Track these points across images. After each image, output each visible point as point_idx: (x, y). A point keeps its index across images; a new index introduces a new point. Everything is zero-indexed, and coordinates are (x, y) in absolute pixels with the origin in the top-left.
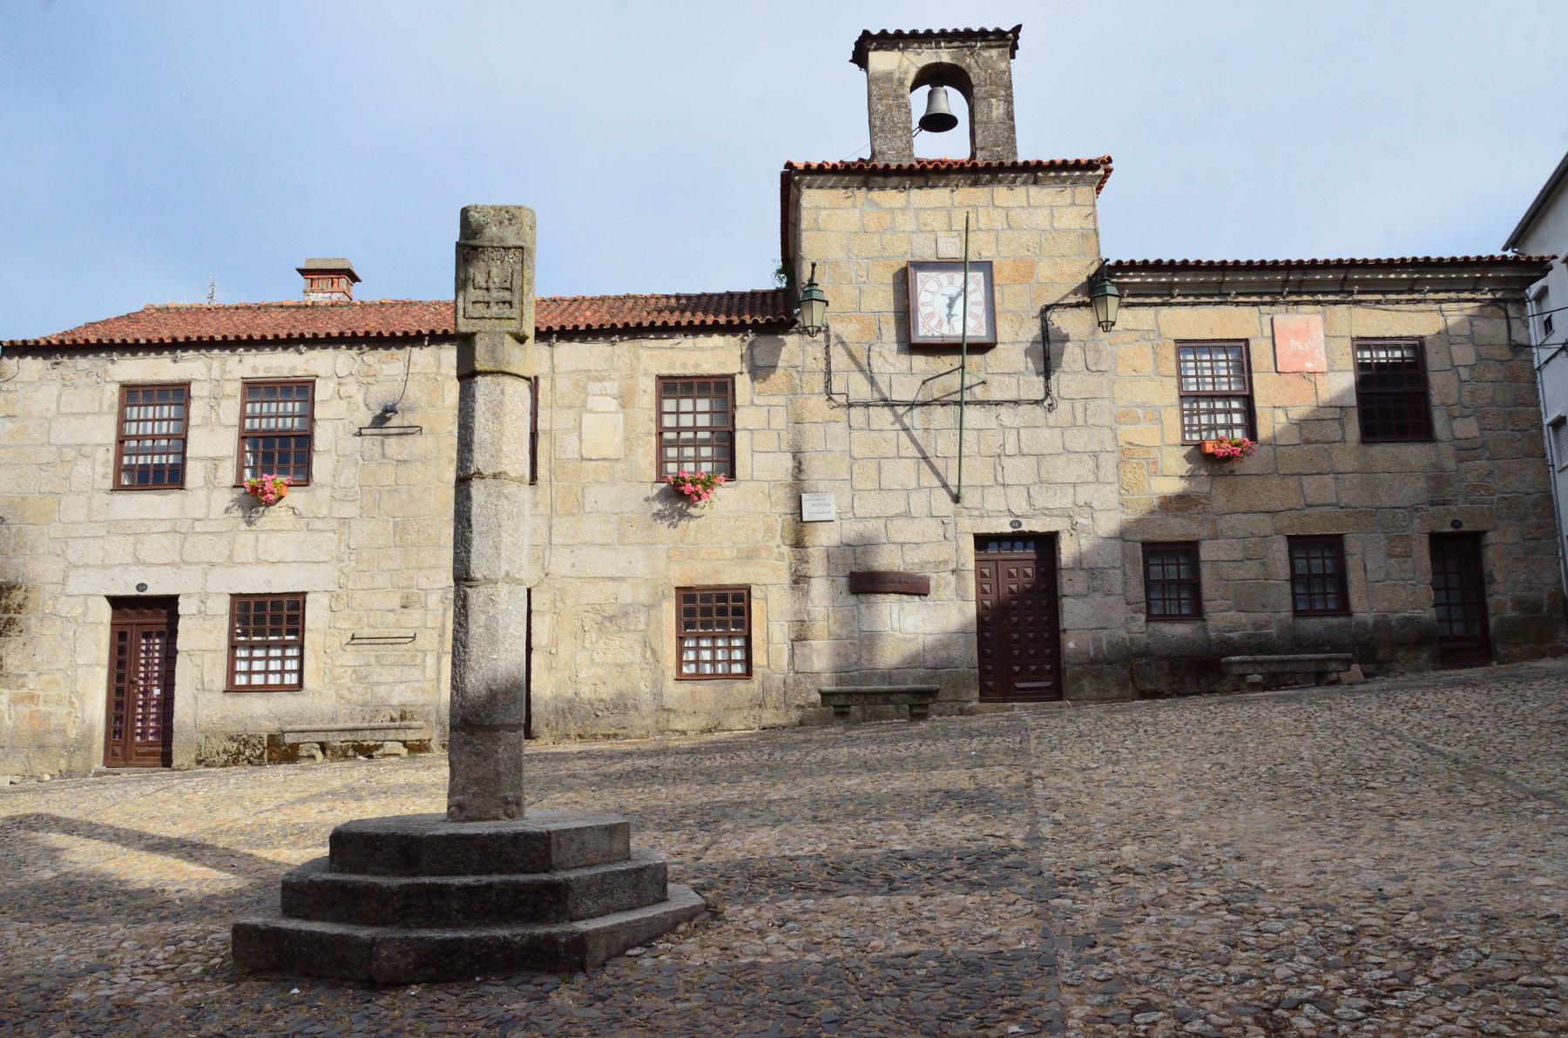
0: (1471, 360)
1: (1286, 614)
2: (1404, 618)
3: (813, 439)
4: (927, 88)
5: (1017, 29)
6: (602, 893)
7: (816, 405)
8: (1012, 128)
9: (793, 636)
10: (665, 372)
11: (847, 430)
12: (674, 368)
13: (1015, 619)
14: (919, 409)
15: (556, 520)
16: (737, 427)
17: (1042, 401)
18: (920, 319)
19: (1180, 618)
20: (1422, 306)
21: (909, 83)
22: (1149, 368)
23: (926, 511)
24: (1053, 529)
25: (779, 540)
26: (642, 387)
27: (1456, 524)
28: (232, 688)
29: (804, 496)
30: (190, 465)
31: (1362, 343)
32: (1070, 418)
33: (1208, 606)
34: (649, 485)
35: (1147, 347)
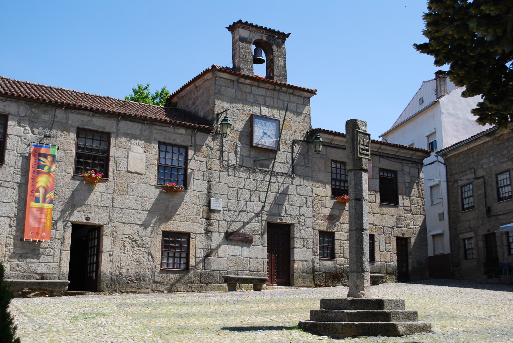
0: (409, 181)
8: (286, 71)
12: (166, 140)
18: (255, 137)
20: (397, 161)
22: (323, 169)
24: (292, 223)
31: (381, 170)
34: (154, 187)
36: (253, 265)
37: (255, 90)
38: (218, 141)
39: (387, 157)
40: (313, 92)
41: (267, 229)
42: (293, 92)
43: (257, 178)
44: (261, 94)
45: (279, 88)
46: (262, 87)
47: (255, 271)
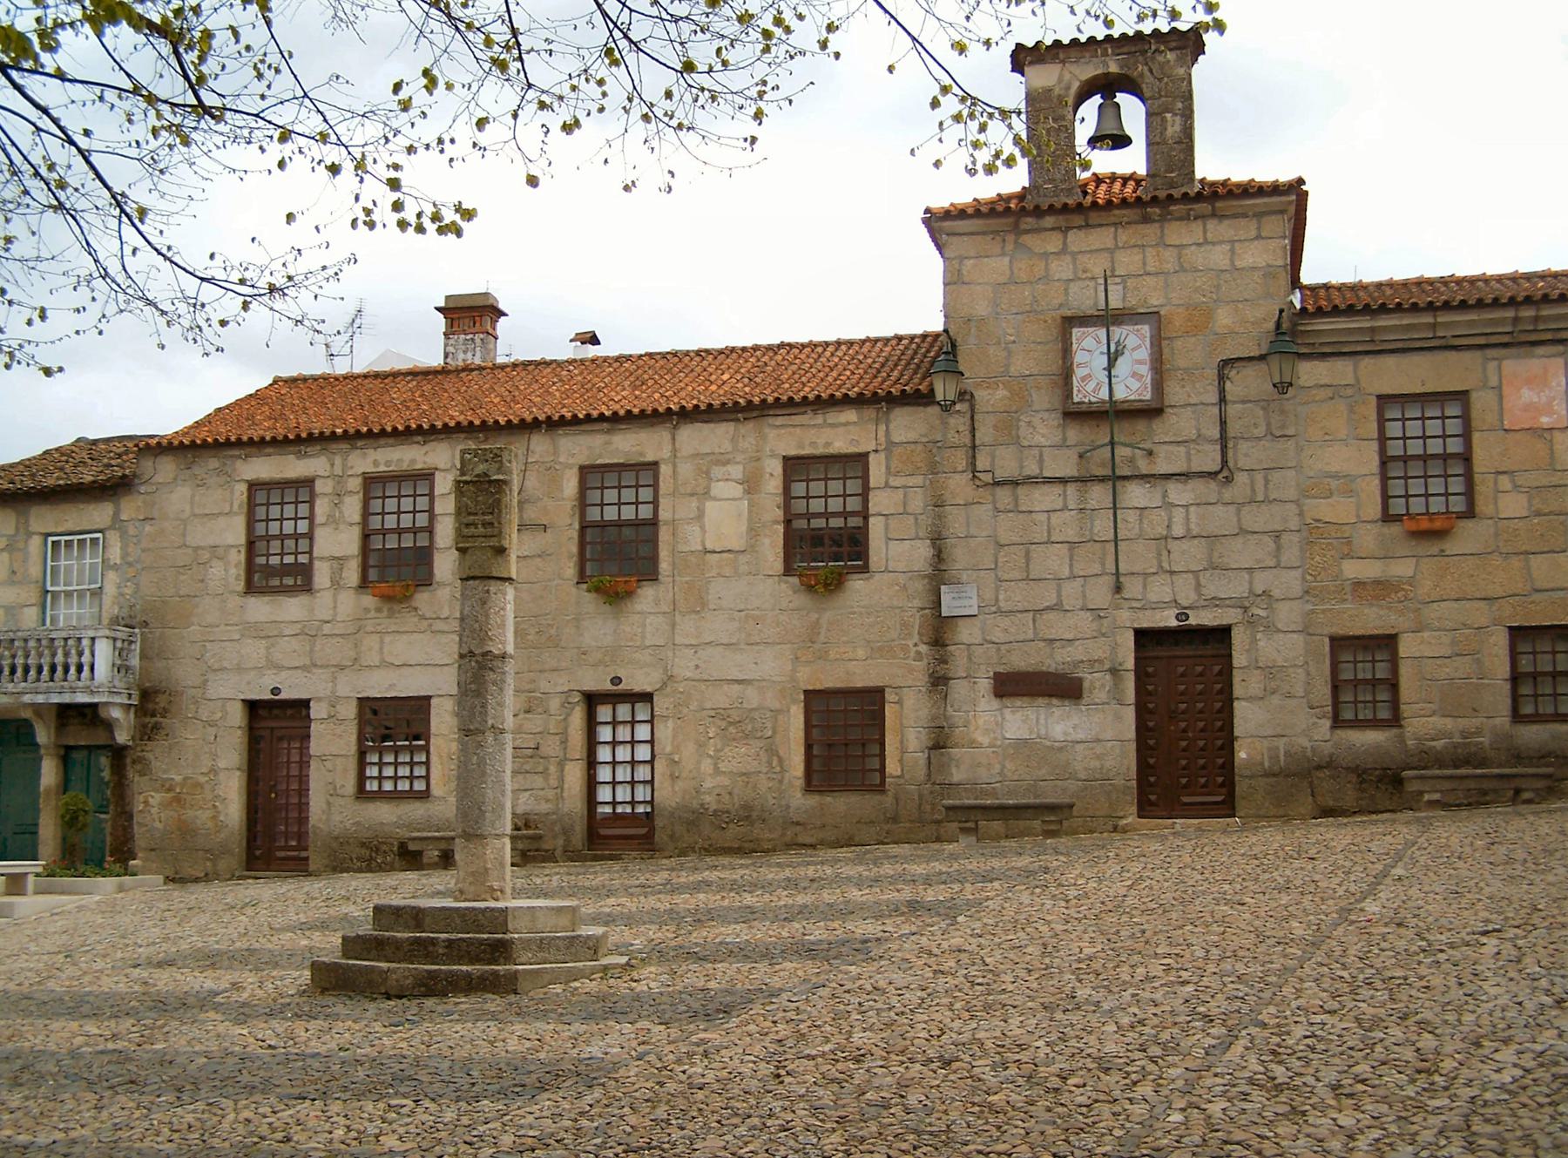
1: (1503, 720)
3: (956, 523)
4: (1097, 100)
6: (541, 948)
7: (958, 485)
9: (930, 744)
10: (793, 452)
11: (990, 513)
12: (803, 448)
13: (1183, 725)
14: (1074, 485)
15: (678, 618)
16: (871, 512)
17: (1216, 473)
19: (1375, 724)
21: (1071, 101)
23: (1079, 603)
25: (916, 638)
26: (768, 470)
28: (362, 793)
29: (943, 587)
30: (317, 564)
32: (1249, 492)
33: (1405, 710)
35: (1341, 406)
36: (1082, 762)
37: (1077, 240)
38: (959, 422)
41: (1137, 651)
42: (1213, 207)
43: (1093, 504)
45: (1157, 210)
46: (1101, 225)
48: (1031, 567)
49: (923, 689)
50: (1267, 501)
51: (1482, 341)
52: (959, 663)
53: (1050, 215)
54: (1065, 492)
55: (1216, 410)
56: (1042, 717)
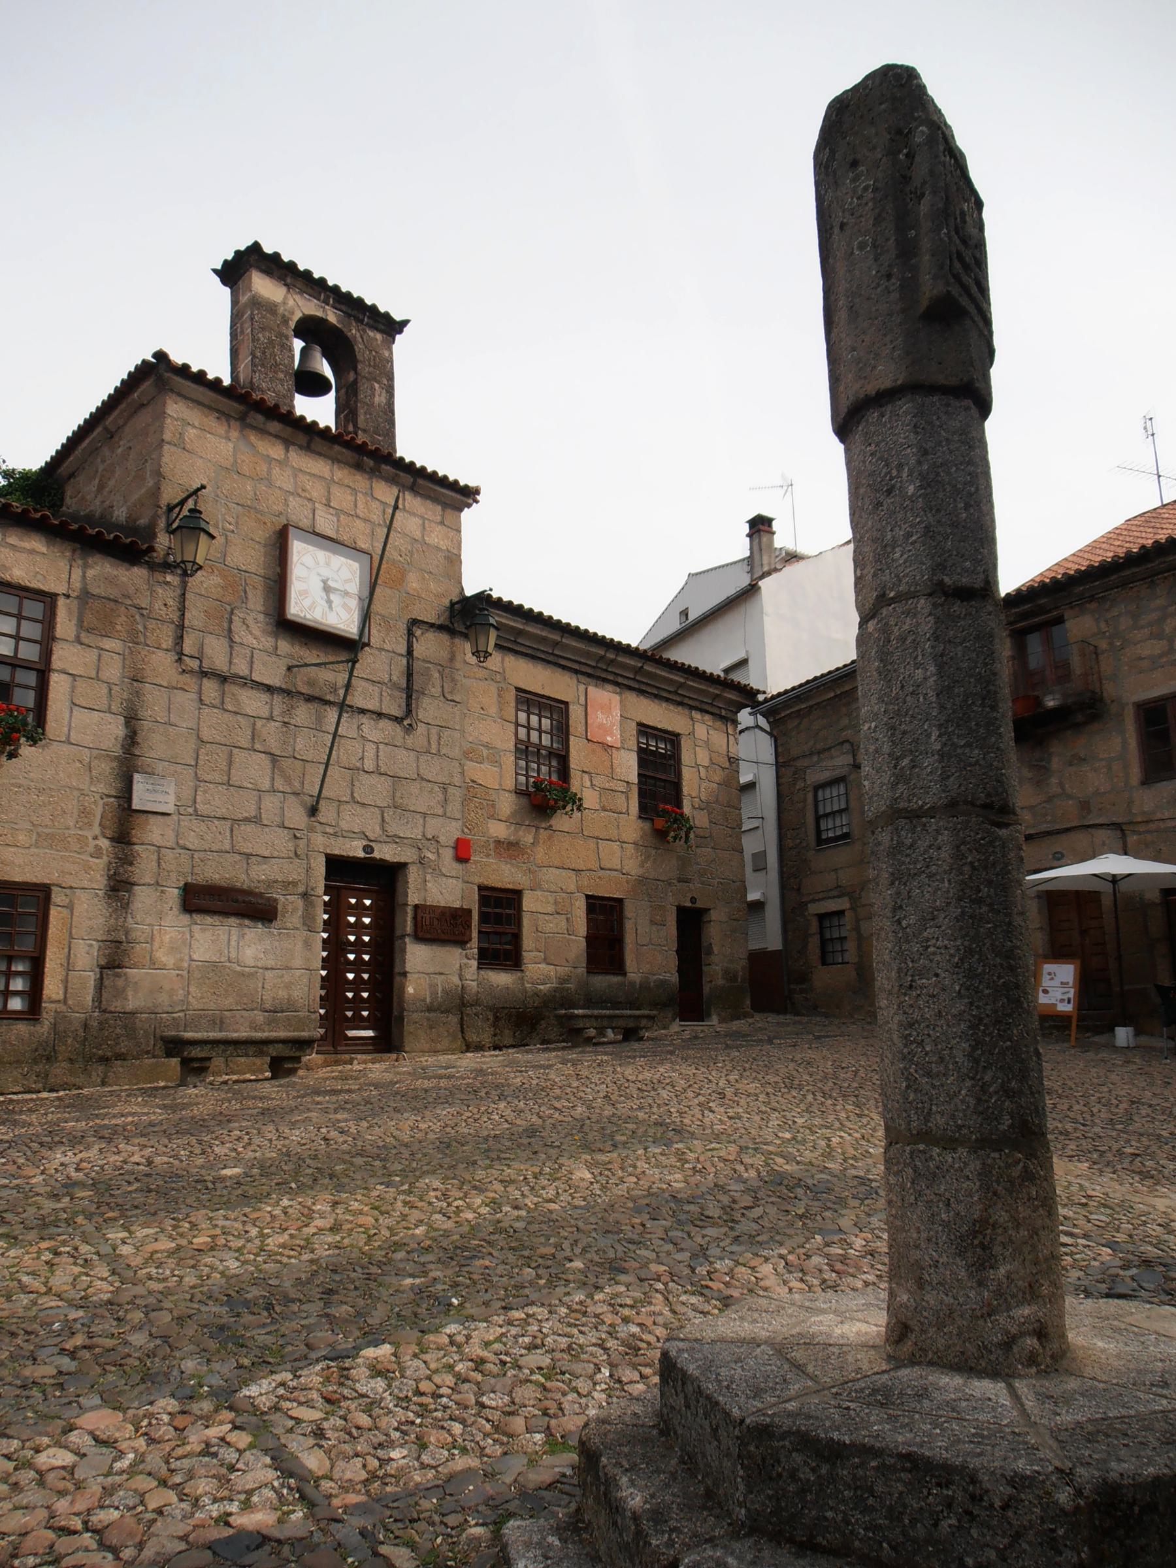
2: (661, 981)
3: (154, 705)
5: (405, 323)
7: (161, 664)
11: (196, 704)
20: (680, 708)
22: (493, 710)
23: (278, 820)
25: (97, 830)
27: (693, 900)
29: (136, 776)
32: (426, 744)
36: (272, 989)
37: (297, 458)
39: (656, 696)
40: (467, 495)
41: (326, 879)
42: (414, 483)
43: (298, 720)
44: (315, 471)
45: (371, 463)
46: (320, 454)
47: (282, 1012)
48: (232, 771)
49: (101, 893)
50: (438, 754)
51: (576, 666)
52: (145, 867)
53: (279, 421)
54: (272, 700)
55: (404, 661)
56: (234, 938)
